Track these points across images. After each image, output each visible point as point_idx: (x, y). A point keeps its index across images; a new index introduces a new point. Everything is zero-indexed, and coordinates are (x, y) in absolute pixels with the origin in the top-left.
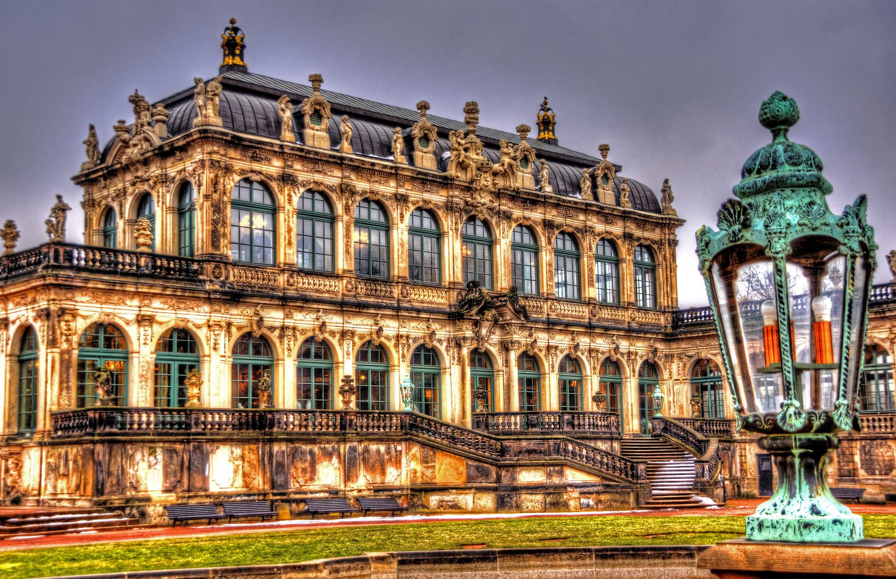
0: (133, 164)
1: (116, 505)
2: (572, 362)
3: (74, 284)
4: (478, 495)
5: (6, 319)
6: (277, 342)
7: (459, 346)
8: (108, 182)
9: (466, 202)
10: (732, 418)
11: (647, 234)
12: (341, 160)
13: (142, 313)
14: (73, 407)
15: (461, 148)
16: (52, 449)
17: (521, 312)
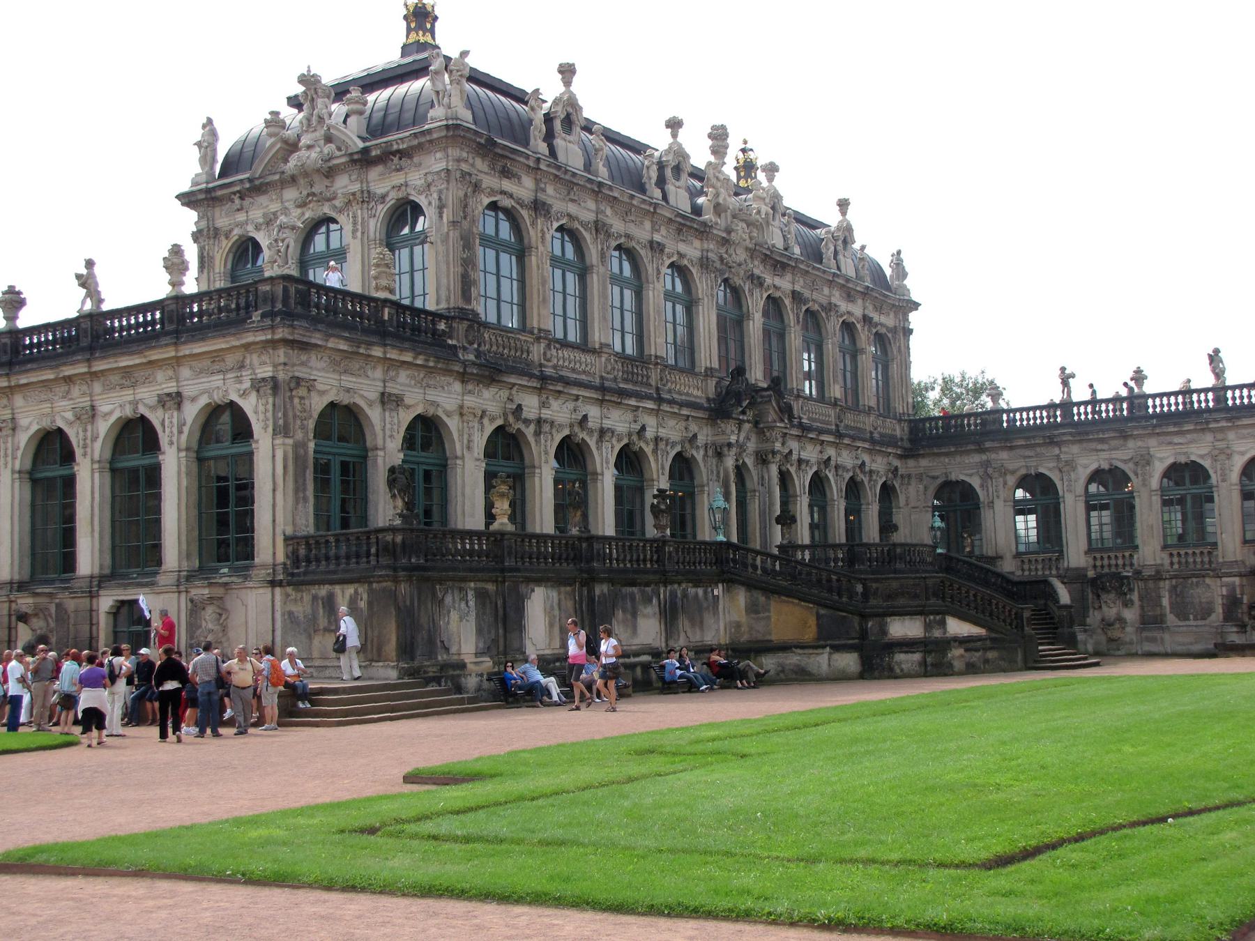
0: (306, 174)
1: (431, 674)
2: (818, 485)
3: (313, 341)
4: (836, 656)
5: (179, 394)
6: (531, 439)
7: (719, 455)
8: (247, 201)
9: (721, 259)
10: (994, 555)
11: (883, 319)
12: (599, 187)
13: (387, 390)
14: (311, 530)
15: (719, 184)
16: (297, 591)
17: (786, 411)
